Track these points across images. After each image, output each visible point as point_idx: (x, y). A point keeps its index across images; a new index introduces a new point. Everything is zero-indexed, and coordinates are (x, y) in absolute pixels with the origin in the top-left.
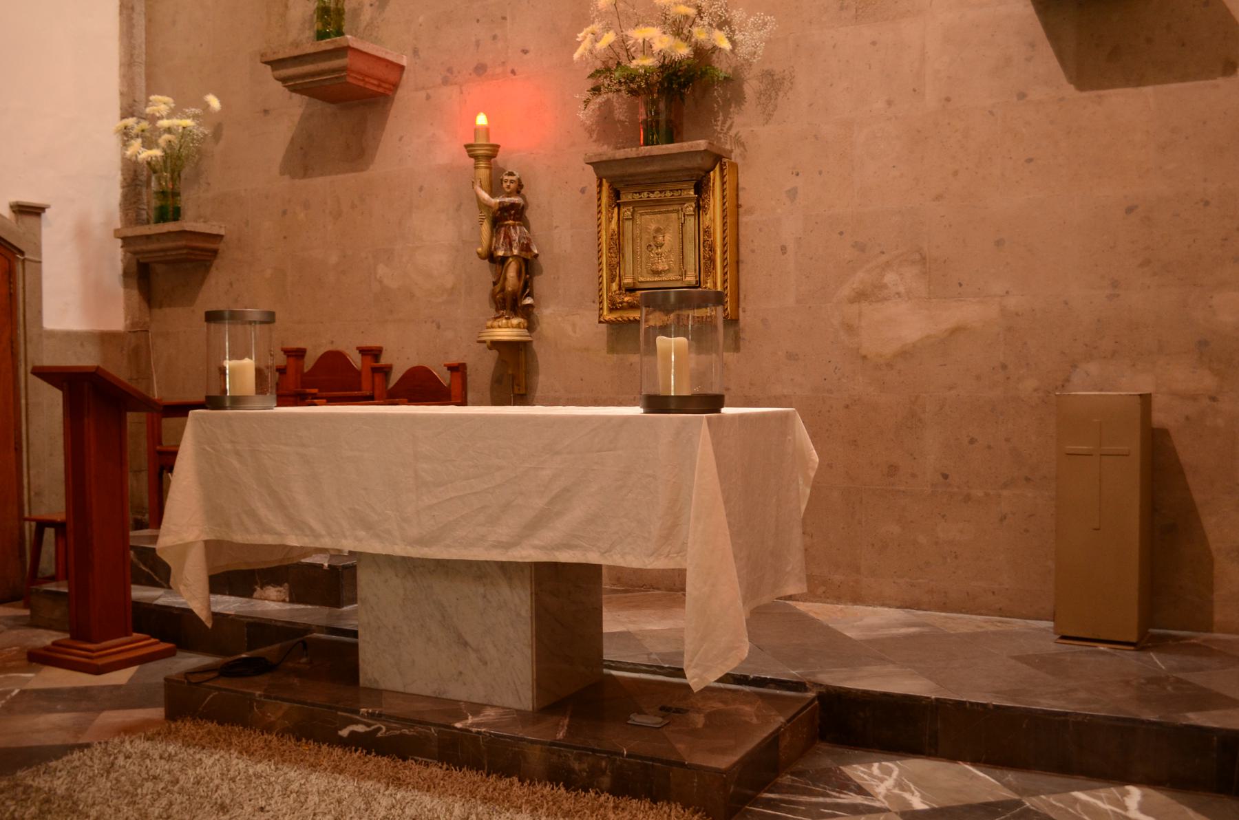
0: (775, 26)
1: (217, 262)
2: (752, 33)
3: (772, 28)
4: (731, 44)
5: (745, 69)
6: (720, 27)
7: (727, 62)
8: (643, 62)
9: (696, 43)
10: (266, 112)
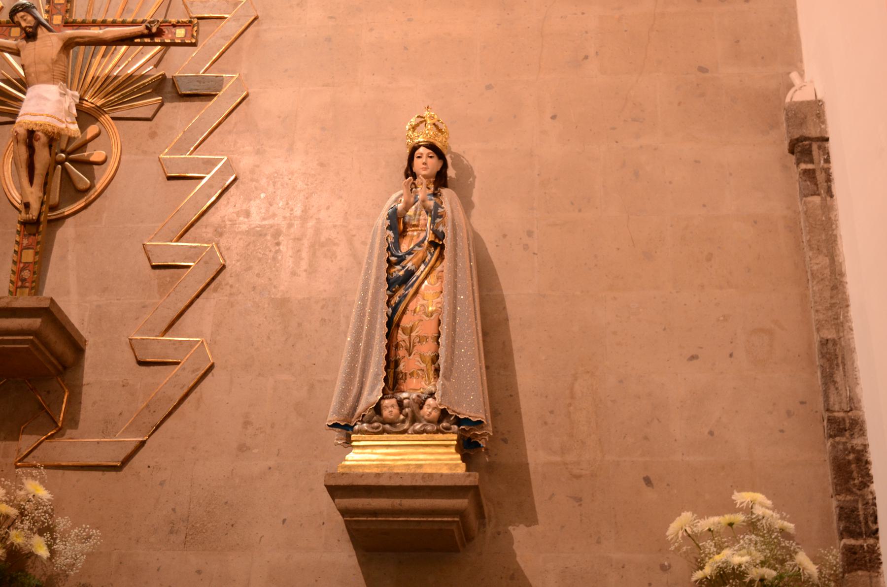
0: (99, 540)
2: (73, 544)
3: (96, 543)
4: (50, 552)
5: (60, 579)
6: (41, 533)
7: (42, 569)
9: (12, 544)
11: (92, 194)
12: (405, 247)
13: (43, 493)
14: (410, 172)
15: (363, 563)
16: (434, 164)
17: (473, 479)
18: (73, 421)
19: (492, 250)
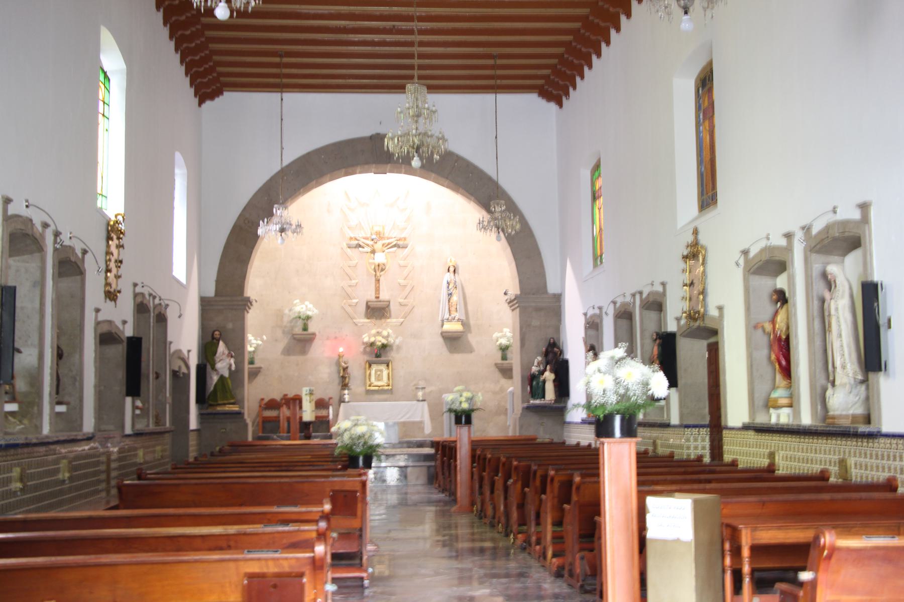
8: (379, 344)
10: (276, 340)
11: (386, 270)
12: (450, 287)
14: (449, 270)
15: (445, 342)
16: (453, 269)
19: (463, 282)
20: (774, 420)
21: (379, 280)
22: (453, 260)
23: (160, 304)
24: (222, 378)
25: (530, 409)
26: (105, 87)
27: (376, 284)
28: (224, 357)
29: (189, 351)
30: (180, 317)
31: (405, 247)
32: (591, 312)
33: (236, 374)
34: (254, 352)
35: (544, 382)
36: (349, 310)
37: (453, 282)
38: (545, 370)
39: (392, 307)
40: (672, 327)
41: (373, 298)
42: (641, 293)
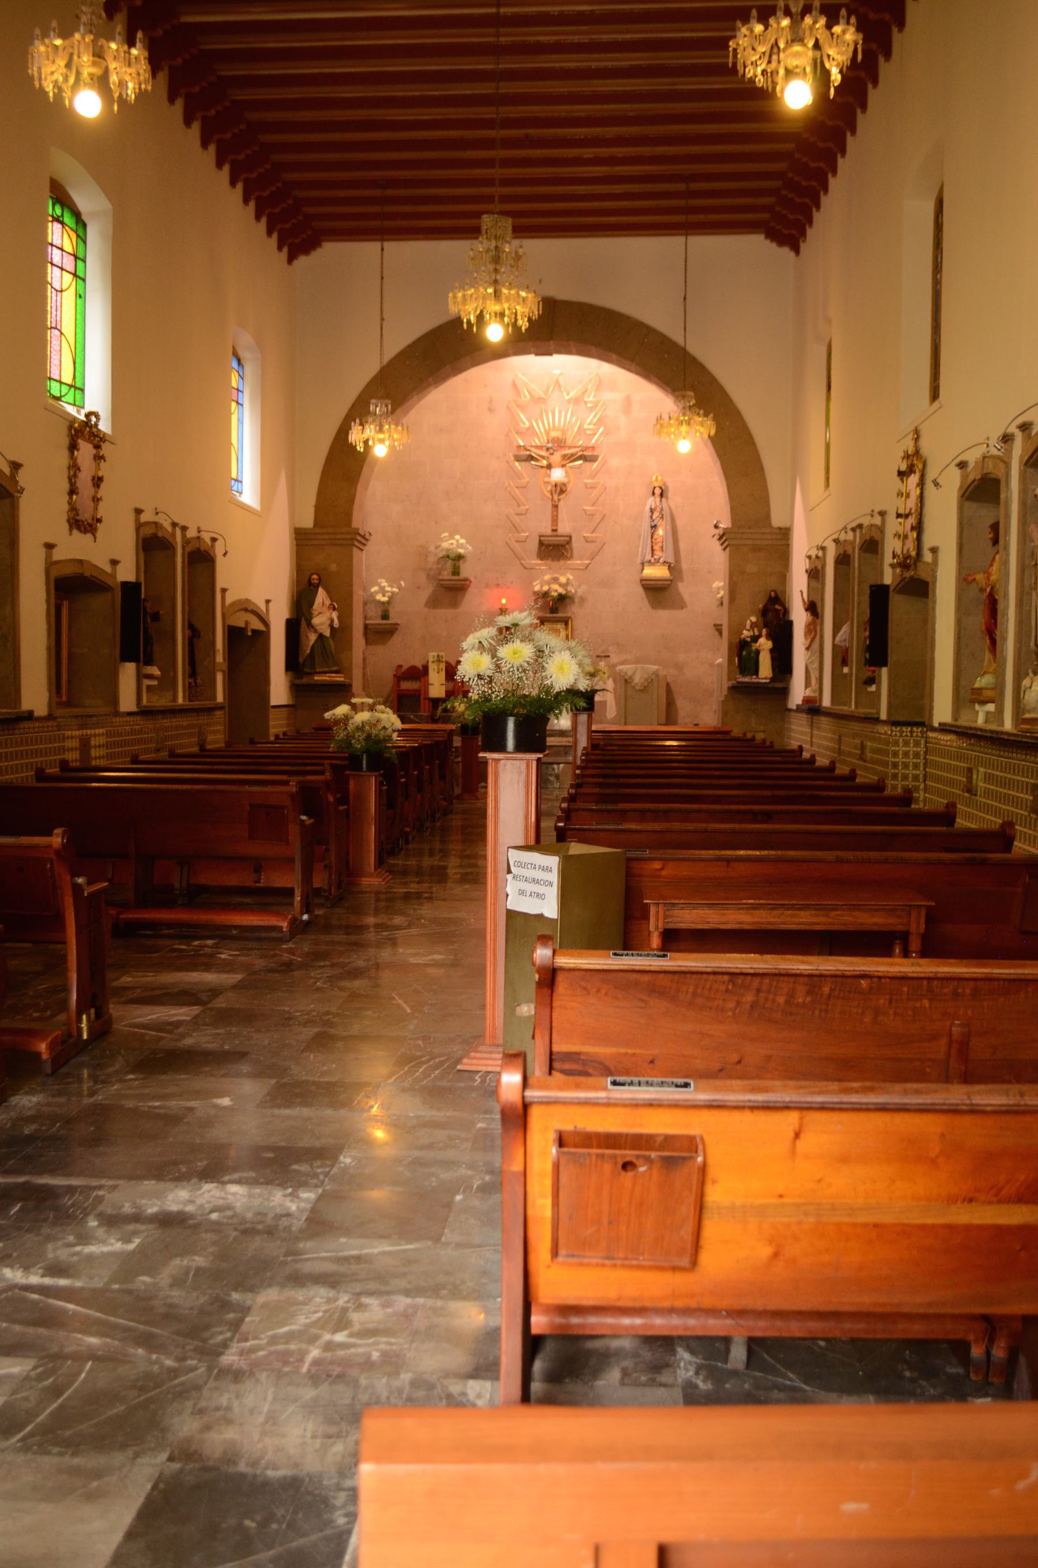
1: (397, 632)
8: (555, 594)
12: (654, 517)
13: (571, 577)
14: (653, 494)
16: (660, 491)
17: (671, 578)
18: (572, 556)
20: (980, 720)
21: (557, 506)
22: (660, 478)
23: (198, 538)
24: (321, 636)
25: (737, 690)
26: (78, 236)
27: (552, 512)
28: (325, 609)
29: (268, 602)
30: (225, 554)
31: (593, 459)
32: (813, 553)
33: (341, 633)
34: (388, 602)
35: (758, 652)
36: (517, 546)
37: (658, 509)
38: (760, 636)
39: (575, 544)
40: (888, 579)
41: (549, 532)
42: (860, 526)
